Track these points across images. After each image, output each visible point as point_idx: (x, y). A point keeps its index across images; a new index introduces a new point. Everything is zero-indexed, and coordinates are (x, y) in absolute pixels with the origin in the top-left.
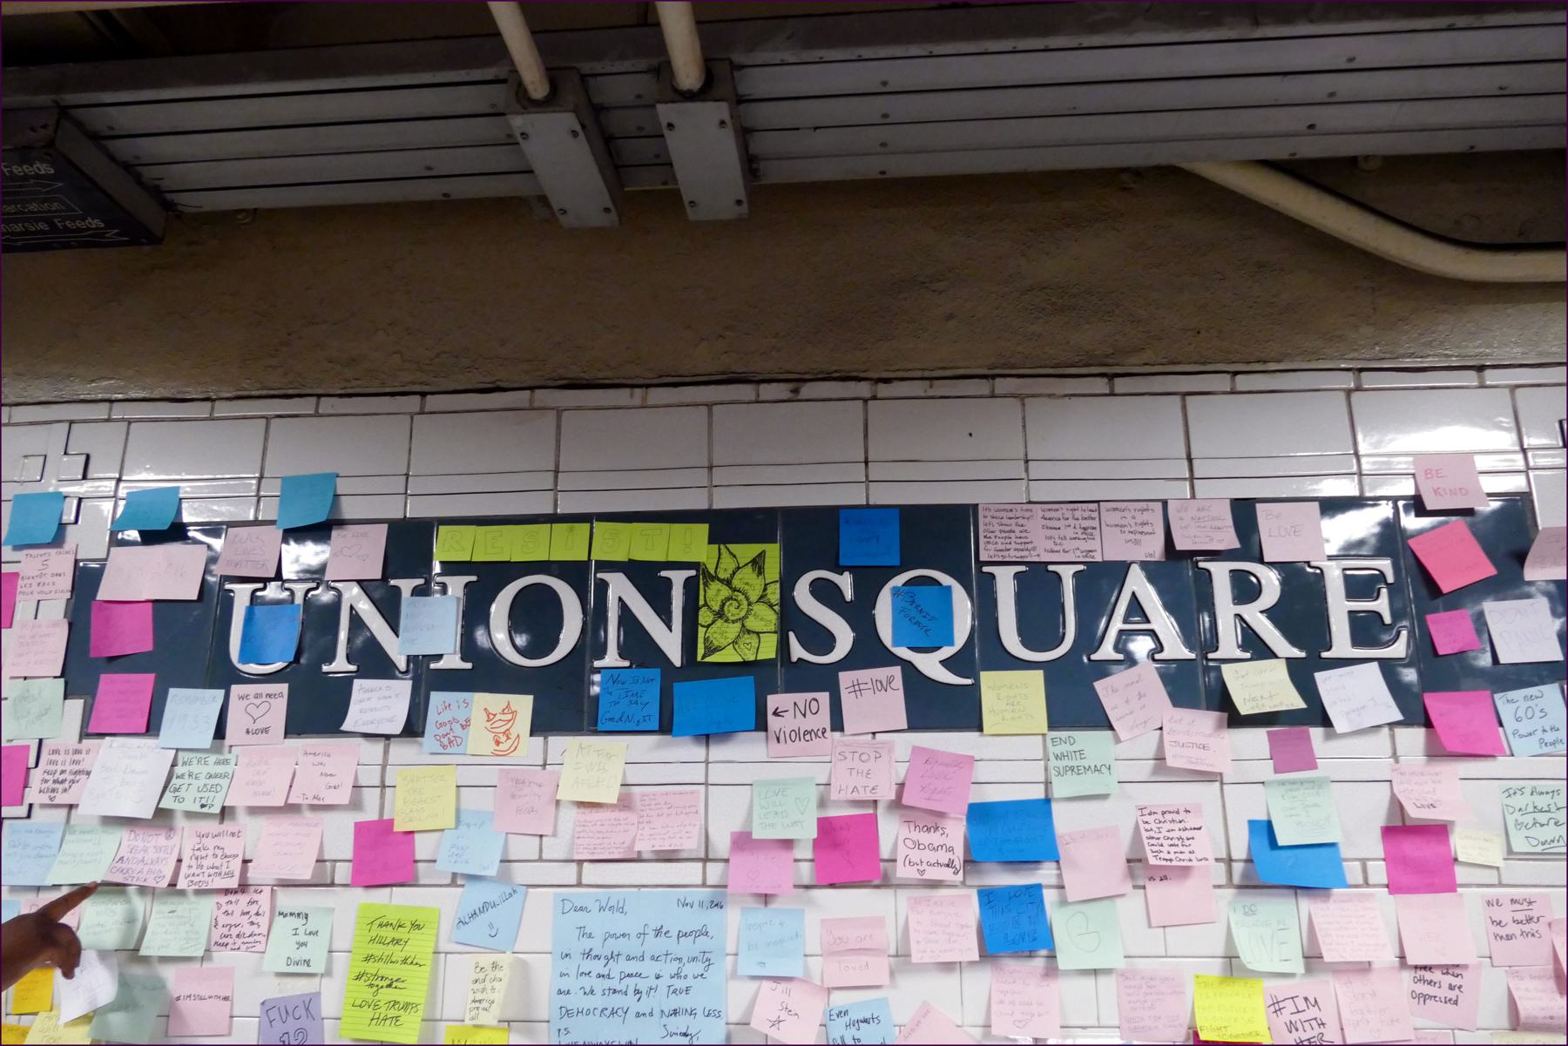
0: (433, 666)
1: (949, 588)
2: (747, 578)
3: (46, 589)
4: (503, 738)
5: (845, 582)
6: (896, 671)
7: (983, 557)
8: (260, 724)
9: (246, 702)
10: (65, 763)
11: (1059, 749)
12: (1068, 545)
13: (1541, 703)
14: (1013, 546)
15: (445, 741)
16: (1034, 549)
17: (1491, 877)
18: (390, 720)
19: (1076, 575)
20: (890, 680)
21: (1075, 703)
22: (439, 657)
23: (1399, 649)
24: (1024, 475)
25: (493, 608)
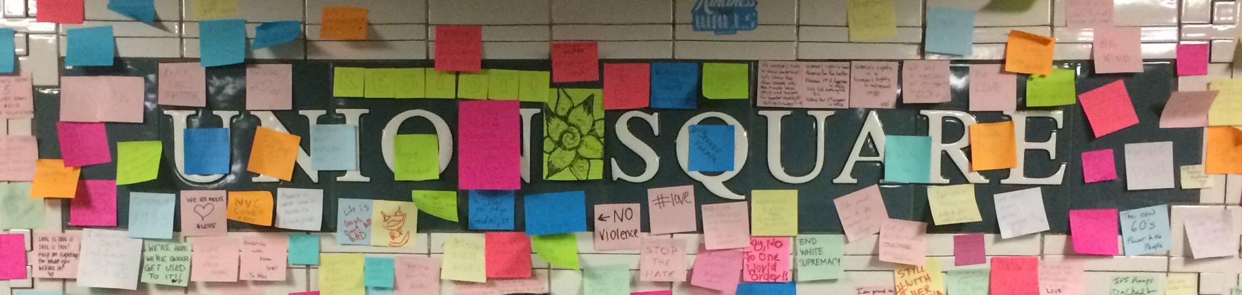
0: (339, 179)
1: (733, 127)
2: (579, 115)
3: (13, 110)
4: (397, 234)
5: (653, 120)
6: (690, 189)
7: (759, 104)
8: (207, 221)
9: (193, 204)
10: (53, 247)
11: (807, 246)
12: (825, 95)
13: (1152, 218)
14: (783, 95)
15: (353, 235)
16: (798, 98)
18: (311, 219)
19: (828, 118)
20: (686, 195)
21: (818, 216)
22: (343, 173)
23: (1057, 179)
24: (795, 38)
25: (385, 132)
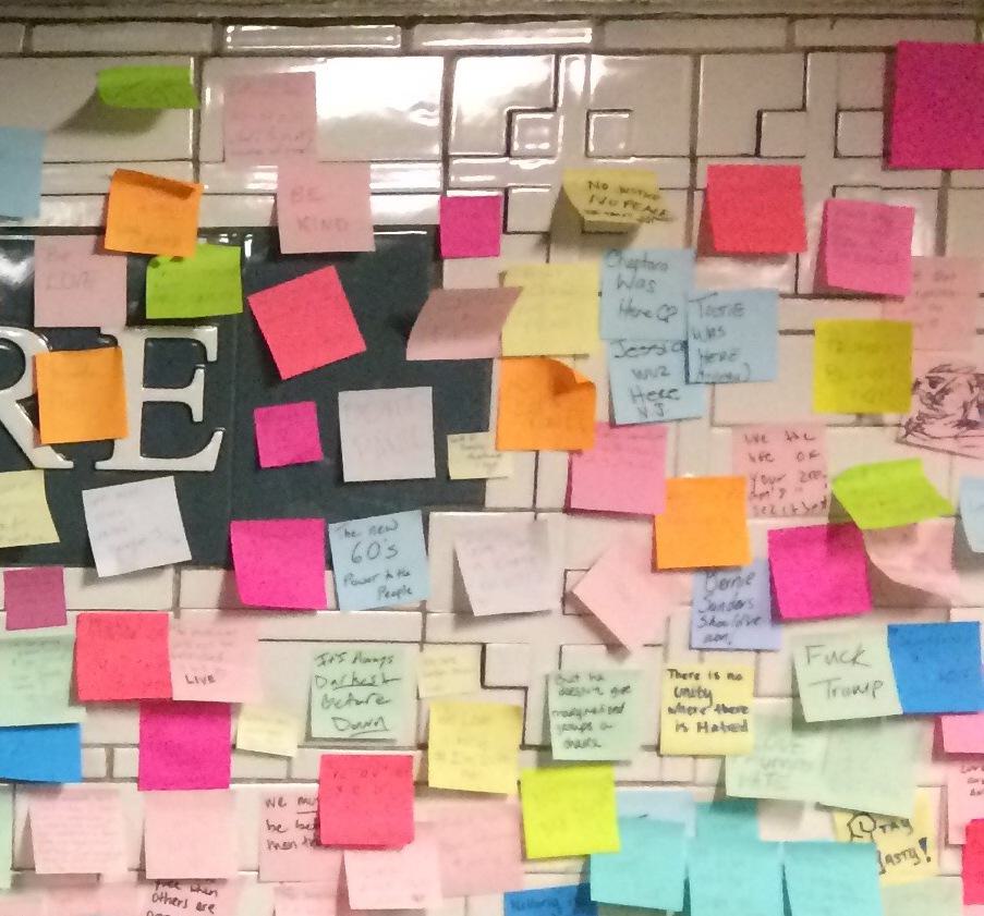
17: (279, 769)
23: (206, 460)
